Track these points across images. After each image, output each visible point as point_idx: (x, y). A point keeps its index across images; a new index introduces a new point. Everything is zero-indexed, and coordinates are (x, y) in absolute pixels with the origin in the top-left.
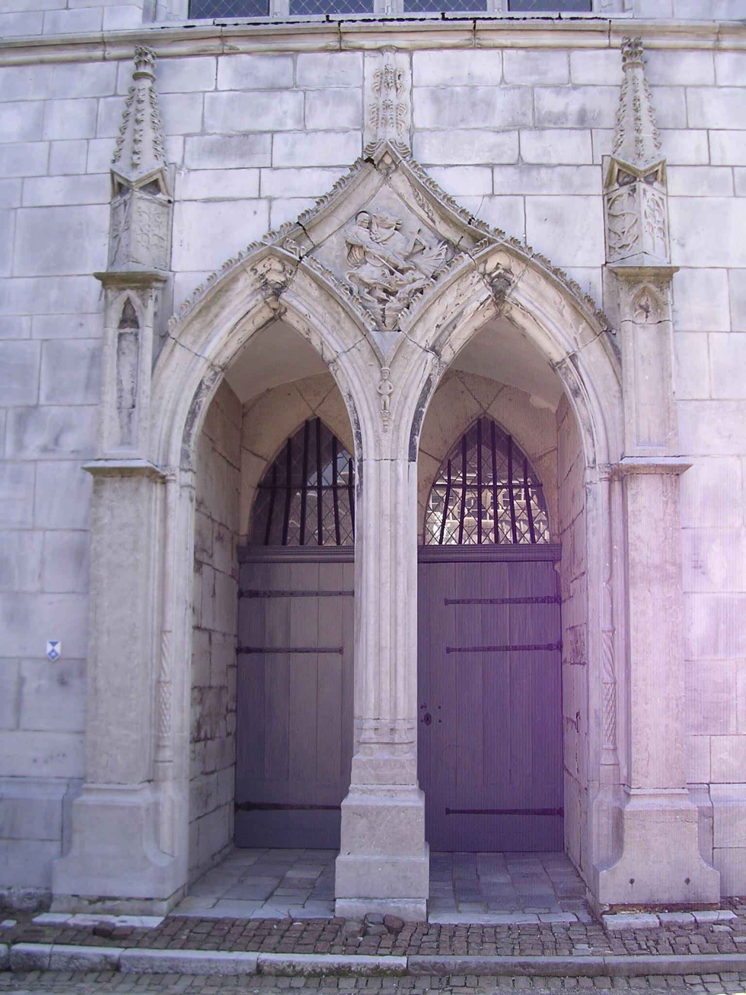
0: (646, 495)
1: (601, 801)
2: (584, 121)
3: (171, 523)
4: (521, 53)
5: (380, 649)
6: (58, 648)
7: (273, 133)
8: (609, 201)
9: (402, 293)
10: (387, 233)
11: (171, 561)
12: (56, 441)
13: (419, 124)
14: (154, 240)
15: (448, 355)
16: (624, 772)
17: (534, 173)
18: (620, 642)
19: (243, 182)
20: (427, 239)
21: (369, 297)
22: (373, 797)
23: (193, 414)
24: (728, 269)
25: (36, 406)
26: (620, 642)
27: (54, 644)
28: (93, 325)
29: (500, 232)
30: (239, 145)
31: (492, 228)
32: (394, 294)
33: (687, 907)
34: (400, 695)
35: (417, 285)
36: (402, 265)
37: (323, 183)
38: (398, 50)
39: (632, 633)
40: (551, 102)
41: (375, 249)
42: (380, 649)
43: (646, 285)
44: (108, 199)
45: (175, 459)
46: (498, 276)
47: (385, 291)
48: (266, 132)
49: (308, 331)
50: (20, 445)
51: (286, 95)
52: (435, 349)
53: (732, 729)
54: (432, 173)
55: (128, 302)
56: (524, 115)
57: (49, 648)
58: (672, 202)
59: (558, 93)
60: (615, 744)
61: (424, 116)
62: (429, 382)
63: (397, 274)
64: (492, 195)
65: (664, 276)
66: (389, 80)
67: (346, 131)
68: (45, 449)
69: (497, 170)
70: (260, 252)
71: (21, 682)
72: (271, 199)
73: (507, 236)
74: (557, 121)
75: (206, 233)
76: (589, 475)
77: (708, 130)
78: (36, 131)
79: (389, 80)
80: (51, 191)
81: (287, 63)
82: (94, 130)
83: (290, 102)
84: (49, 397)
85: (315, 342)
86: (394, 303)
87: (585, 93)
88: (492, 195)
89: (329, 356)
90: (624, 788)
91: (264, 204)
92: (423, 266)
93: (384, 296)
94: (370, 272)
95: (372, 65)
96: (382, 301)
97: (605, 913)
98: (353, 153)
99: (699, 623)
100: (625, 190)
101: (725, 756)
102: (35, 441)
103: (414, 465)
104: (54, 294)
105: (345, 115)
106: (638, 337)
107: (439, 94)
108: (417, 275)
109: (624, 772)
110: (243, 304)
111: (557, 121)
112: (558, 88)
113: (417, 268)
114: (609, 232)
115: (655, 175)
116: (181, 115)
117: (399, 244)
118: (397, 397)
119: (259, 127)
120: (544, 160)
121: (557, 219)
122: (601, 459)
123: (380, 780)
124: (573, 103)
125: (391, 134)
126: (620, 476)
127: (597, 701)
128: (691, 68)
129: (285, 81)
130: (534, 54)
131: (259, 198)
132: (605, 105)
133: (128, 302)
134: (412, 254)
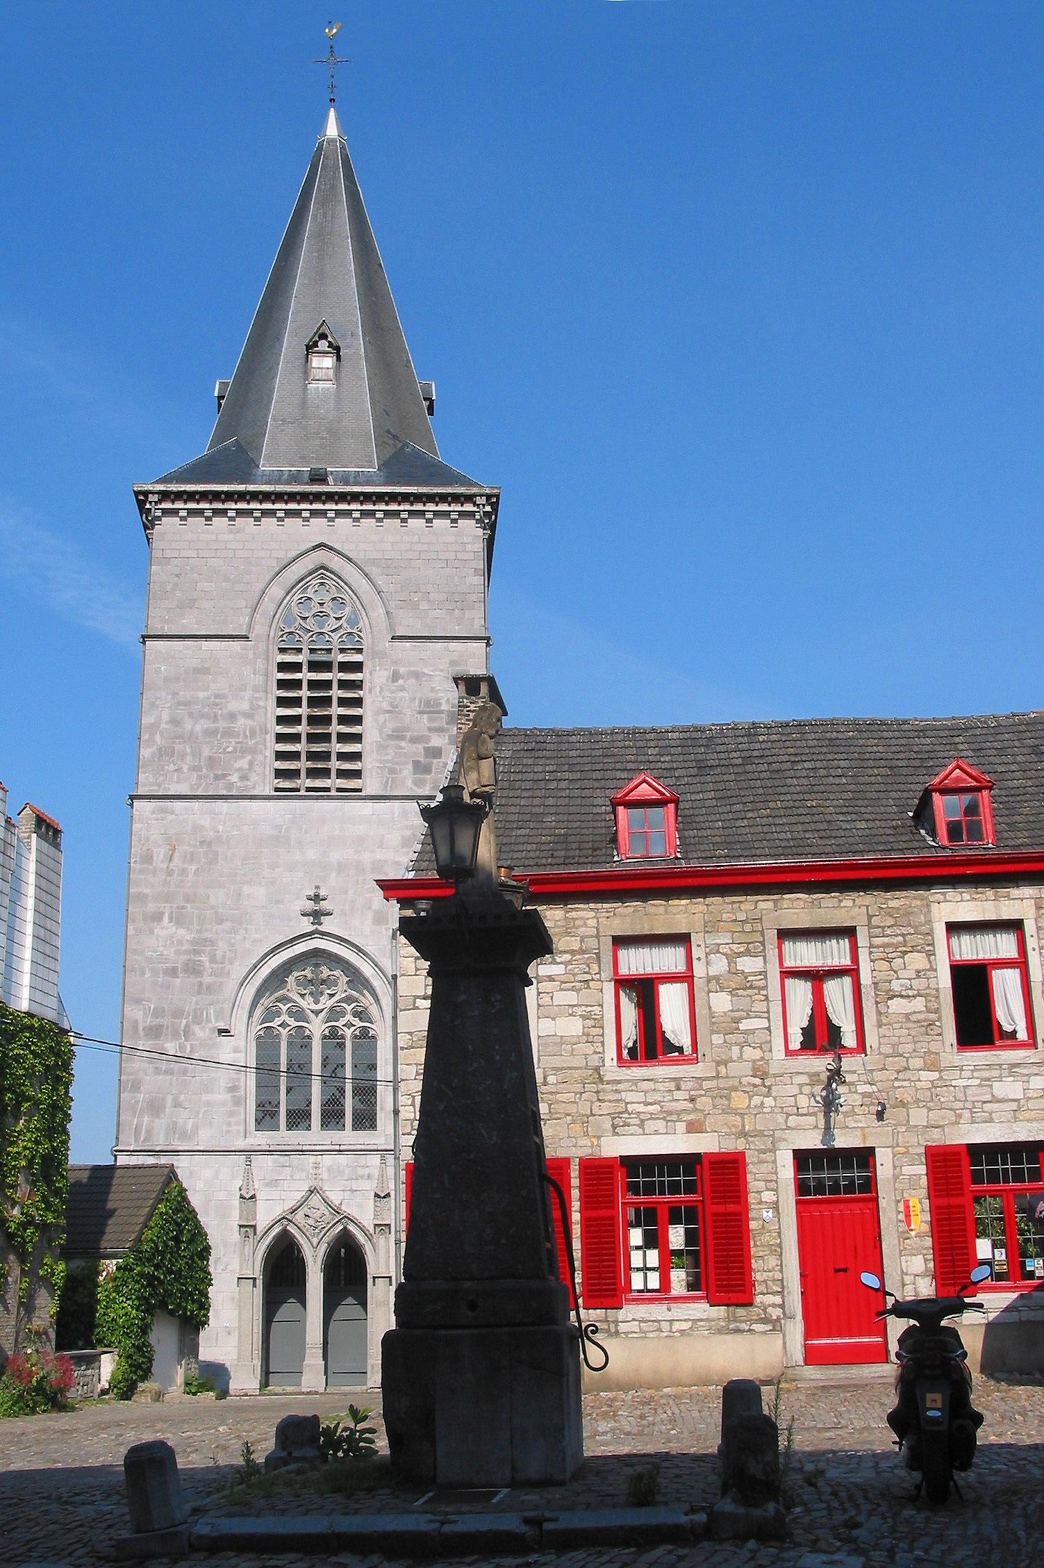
19: (276, 1195)
20: (326, 1212)
30: (273, 1183)
37: (299, 1196)
40: (360, 1171)
61: (325, 1176)
74: (362, 1177)
75: (265, 1215)
78: (216, 1176)
80: (222, 1195)
94: (311, 1222)
105: (304, 1175)
107: (329, 1169)
117: (319, 1213)
121: (361, 1206)
124: (367, 1171)
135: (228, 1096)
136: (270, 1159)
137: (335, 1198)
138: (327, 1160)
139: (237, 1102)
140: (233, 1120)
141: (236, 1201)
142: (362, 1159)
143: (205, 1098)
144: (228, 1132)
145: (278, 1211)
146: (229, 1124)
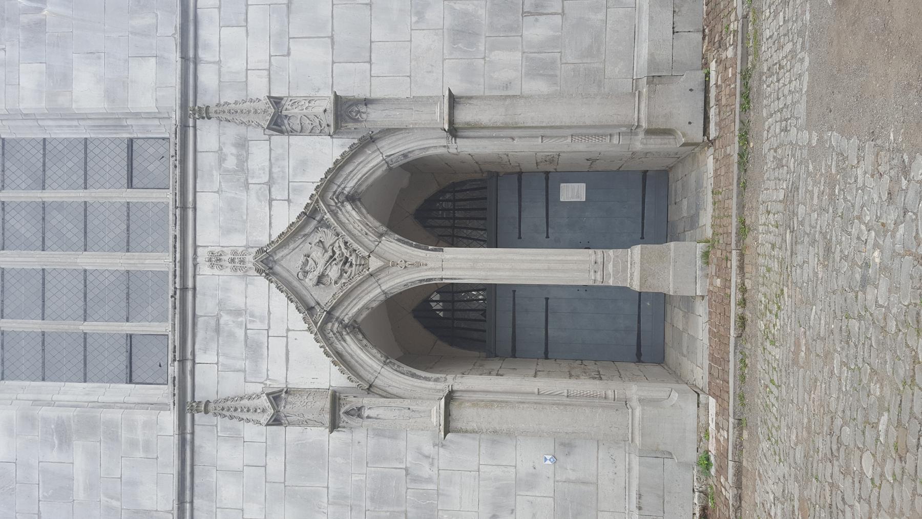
0: (464, 115)
1: (639, 143)
2: (242, 144)
3: (476, 388)
4: (198, 181)
5: (549, 270)
6: (548, 457)
7: (246, 329)
8: (292, 132)
9: (346, 253)
10: (311, 261)
11: (498, 389)
12: (427, 457)
13: (244, 243)
14: (311, 398)
15: (383, 229)
16: (624, 129)
17: (275, 176)
18: (548, 132)
19: (277, 347)
20: (315, 238)
21: (349, 273)
22: (635, 274)
23: (413, 375)
24: (333, 63)
25: (406, 469)
26: (548, 132)
27: (546, 459)
28: (360, 435)
29: (312, 196)
30: (254, 349)
31: (309, 202)
32: (347, 259)
33: (706, 90)
34: (575, 258)
35: (343, 246)
36: (330, 253)
37: (280, 300)
38: (195, 253)
39: (544, 125)
40: (231, 163)
41: (320, 269)
42: (549, 270)
43: (345, 111)
44: (282, 428)
45: (440, 386)
46: (337, 198)
47: (345, 263)
48: (246, 333)
49: (368, 308)
50: (429, 480)
51: (222, 321)
52: (381, 235)
53: (601, 66)
54: (274, 238)
55: (347, 413)
56: (238, 180)
57: (548, 462)
58: (293, 94)
59: (225, 160)
60: (606, 136)
61: (238, 241)
62: (399, 240)
63: (336, 256)
64: (289, 200)
65: (338, 101)
66: (216, 260)
67: (247, 285)
68: (432, 464)
69: (274, 197)
70: (322, 334)
71: (568, 481)
72: (288, 330)
73: (314, 192)
76: (453, 150)
77: (247, 70)
79: (216, 260)
80: (275, 464)
81: (200, 322)
82: (236, 437)
83: (225, 318)
84: (401, 462)
85: (374, 305)
86: (353, 259)
87: (224, 144)
88: (289, 200)
89: (382, 298)
90: (632, 130)
91: (290, 333)
92: (332, 242)
93: (348, 264)
95: (204, 269)
96: (351, 265)
97: (708, 138)
98: (262, 281)
99: (539, 86)
100: (286, 121)
101: (617, 70)
102: (426, 470)
103: (445, 249)
104: (340, 460)
106: (376, 117)
108: (337, 245)
109: (624, 129)
110: (352, 346)
111: (242, 161)
112: (222, 159)
113: (332, 245)
114: (312, 132)
115: (276, 102)
116: (232, 385)
118: (406, 258)
119: (243, 338)
120: (267, 170)
121: (304, 164)
122: (443, 142)
123: (625, 270)
124: (230, 150)
125: (250, 259)
126: (454, 131)
127: (582, 146)
128: (207, 77)
129: (213, 322)
130: (199, 173)
131: (287, 337)
132: (232, 131)
133: (347, 413)
134: (324, 248)
135: (78, 446)
136: (206, 358)
137: (285, 217)
138: (209, 234)
139: (89, 427)
140: (124, 435)
141: (292, 433)
142: (206, 161)
143: (80, 494)
144: (147, 447)
145: (307, 344)
146: (133, 444)
